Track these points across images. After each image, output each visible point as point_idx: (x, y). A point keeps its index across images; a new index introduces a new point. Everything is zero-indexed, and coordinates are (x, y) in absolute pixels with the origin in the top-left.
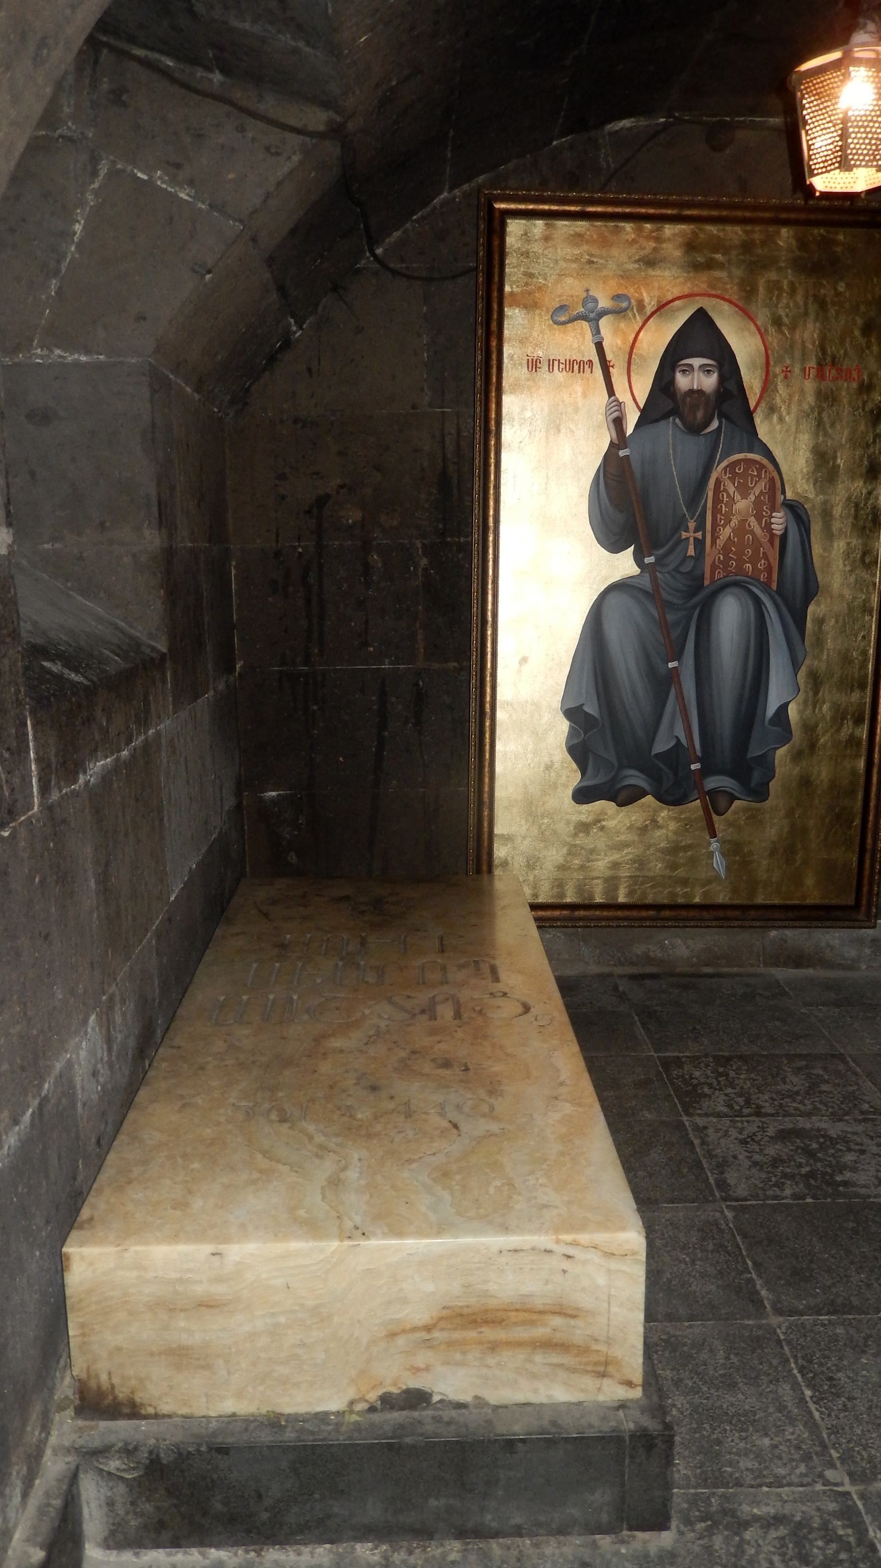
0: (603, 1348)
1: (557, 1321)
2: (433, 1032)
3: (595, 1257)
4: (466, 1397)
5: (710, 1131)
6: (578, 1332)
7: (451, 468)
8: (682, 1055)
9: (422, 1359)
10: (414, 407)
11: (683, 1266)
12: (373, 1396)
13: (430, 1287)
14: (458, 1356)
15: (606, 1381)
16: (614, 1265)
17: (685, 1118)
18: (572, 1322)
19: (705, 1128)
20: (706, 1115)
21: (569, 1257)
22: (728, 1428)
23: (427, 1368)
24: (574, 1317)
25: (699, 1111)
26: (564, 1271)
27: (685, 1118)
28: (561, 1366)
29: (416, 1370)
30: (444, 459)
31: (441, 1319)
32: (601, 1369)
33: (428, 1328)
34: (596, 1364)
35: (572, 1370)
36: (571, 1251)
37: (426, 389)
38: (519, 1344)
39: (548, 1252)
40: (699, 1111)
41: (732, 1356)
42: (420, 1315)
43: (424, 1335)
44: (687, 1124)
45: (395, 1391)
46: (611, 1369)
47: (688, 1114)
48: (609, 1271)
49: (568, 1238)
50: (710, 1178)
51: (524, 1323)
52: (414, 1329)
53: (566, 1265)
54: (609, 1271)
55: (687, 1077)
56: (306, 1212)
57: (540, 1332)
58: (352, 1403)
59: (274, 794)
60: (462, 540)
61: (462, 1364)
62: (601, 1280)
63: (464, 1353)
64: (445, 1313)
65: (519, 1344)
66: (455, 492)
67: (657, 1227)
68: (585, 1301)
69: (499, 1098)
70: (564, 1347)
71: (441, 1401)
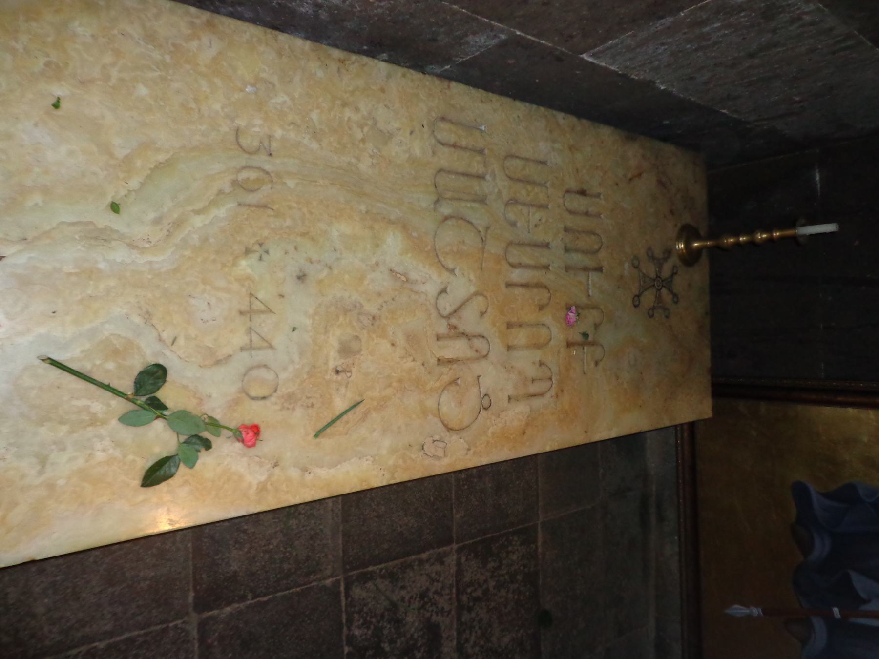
2: (412, 338)
5: (438, 567)
8: (539, 544)
11: (263, 543)
17: (455, 546)
19: (442, 563)
20: (459, 564)
22: (58, 578)
25: (463, 559)
27: (455, 546)
40: (463, 559)
41: (147, 583)
44: (446, 548)
47: (460, 550)
50: (375, 568)
55: (510, 548)
56: (36, 204)
59: (818, 178)
67: (313, 522)
69: (278, 407)
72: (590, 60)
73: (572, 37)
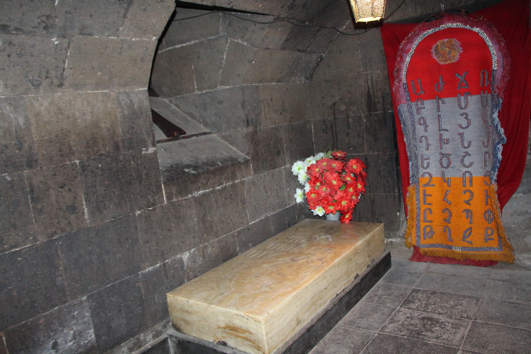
0: (258, 343)
1: (248, 334)
3: (253, 321)
4: (234, 347)
6: (252, 338)
7: (371, 90)
9: (224, 335)
10: (358, 72)
12: (217, 340)
13: (223, 319)
14: (231, 337)
15: (260, 352)
16: (257, 323)
18: (251, 335)
21: (248, 319)
23: (226, 337)
24: (251, 334)
26: (247, 323)
28: (250, 345)
29: (224, 337)
30: (368, 88)
31: (226, 327)
32: (258, 348)
33: (224, 328)
34: (257, 347)
35: (252, 347)
36: (248, 318)
37: (361, 66)
38: (241, 337)
39: (243, 317)
42: (223, 325)
43: (223, 329)
45: (220, 341)
46: (260, 349)
48: (256, 325)
49: (247, 314)
51: (242, 332)
52: (222, 328)
53: (247, 321)
54: (256, 325)
57: (245, 336)
58: (214, 341)
60: (376, 113)
61: (232, 338)
62: (255, 327)
63: (232, 336)
64: (227, 326)
65: (241, 337)
66: (372, 97)
68: (253, 331)
70: (250, 340)
71: (229, 346)
72: (252, 223)
73: (242, 222)
